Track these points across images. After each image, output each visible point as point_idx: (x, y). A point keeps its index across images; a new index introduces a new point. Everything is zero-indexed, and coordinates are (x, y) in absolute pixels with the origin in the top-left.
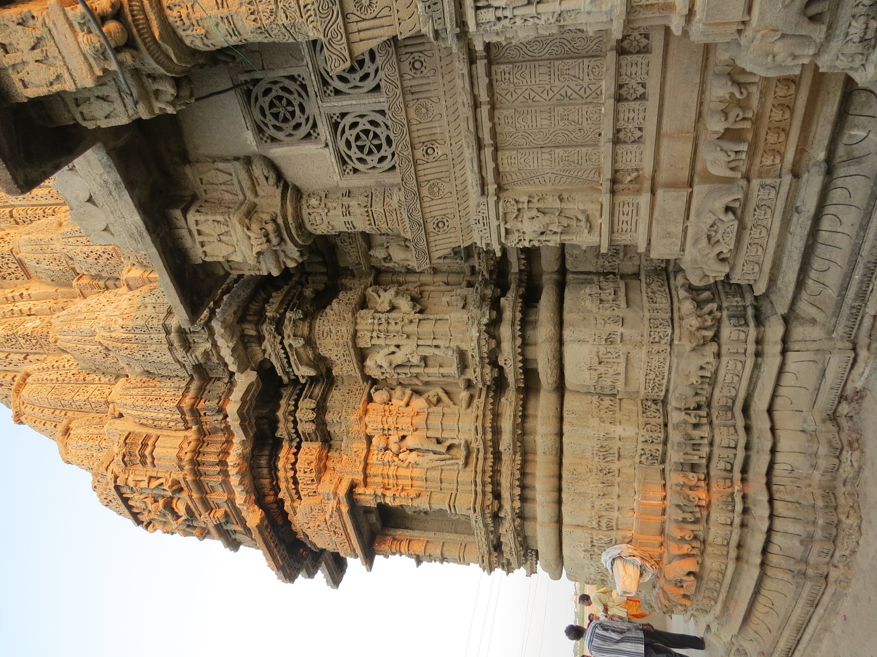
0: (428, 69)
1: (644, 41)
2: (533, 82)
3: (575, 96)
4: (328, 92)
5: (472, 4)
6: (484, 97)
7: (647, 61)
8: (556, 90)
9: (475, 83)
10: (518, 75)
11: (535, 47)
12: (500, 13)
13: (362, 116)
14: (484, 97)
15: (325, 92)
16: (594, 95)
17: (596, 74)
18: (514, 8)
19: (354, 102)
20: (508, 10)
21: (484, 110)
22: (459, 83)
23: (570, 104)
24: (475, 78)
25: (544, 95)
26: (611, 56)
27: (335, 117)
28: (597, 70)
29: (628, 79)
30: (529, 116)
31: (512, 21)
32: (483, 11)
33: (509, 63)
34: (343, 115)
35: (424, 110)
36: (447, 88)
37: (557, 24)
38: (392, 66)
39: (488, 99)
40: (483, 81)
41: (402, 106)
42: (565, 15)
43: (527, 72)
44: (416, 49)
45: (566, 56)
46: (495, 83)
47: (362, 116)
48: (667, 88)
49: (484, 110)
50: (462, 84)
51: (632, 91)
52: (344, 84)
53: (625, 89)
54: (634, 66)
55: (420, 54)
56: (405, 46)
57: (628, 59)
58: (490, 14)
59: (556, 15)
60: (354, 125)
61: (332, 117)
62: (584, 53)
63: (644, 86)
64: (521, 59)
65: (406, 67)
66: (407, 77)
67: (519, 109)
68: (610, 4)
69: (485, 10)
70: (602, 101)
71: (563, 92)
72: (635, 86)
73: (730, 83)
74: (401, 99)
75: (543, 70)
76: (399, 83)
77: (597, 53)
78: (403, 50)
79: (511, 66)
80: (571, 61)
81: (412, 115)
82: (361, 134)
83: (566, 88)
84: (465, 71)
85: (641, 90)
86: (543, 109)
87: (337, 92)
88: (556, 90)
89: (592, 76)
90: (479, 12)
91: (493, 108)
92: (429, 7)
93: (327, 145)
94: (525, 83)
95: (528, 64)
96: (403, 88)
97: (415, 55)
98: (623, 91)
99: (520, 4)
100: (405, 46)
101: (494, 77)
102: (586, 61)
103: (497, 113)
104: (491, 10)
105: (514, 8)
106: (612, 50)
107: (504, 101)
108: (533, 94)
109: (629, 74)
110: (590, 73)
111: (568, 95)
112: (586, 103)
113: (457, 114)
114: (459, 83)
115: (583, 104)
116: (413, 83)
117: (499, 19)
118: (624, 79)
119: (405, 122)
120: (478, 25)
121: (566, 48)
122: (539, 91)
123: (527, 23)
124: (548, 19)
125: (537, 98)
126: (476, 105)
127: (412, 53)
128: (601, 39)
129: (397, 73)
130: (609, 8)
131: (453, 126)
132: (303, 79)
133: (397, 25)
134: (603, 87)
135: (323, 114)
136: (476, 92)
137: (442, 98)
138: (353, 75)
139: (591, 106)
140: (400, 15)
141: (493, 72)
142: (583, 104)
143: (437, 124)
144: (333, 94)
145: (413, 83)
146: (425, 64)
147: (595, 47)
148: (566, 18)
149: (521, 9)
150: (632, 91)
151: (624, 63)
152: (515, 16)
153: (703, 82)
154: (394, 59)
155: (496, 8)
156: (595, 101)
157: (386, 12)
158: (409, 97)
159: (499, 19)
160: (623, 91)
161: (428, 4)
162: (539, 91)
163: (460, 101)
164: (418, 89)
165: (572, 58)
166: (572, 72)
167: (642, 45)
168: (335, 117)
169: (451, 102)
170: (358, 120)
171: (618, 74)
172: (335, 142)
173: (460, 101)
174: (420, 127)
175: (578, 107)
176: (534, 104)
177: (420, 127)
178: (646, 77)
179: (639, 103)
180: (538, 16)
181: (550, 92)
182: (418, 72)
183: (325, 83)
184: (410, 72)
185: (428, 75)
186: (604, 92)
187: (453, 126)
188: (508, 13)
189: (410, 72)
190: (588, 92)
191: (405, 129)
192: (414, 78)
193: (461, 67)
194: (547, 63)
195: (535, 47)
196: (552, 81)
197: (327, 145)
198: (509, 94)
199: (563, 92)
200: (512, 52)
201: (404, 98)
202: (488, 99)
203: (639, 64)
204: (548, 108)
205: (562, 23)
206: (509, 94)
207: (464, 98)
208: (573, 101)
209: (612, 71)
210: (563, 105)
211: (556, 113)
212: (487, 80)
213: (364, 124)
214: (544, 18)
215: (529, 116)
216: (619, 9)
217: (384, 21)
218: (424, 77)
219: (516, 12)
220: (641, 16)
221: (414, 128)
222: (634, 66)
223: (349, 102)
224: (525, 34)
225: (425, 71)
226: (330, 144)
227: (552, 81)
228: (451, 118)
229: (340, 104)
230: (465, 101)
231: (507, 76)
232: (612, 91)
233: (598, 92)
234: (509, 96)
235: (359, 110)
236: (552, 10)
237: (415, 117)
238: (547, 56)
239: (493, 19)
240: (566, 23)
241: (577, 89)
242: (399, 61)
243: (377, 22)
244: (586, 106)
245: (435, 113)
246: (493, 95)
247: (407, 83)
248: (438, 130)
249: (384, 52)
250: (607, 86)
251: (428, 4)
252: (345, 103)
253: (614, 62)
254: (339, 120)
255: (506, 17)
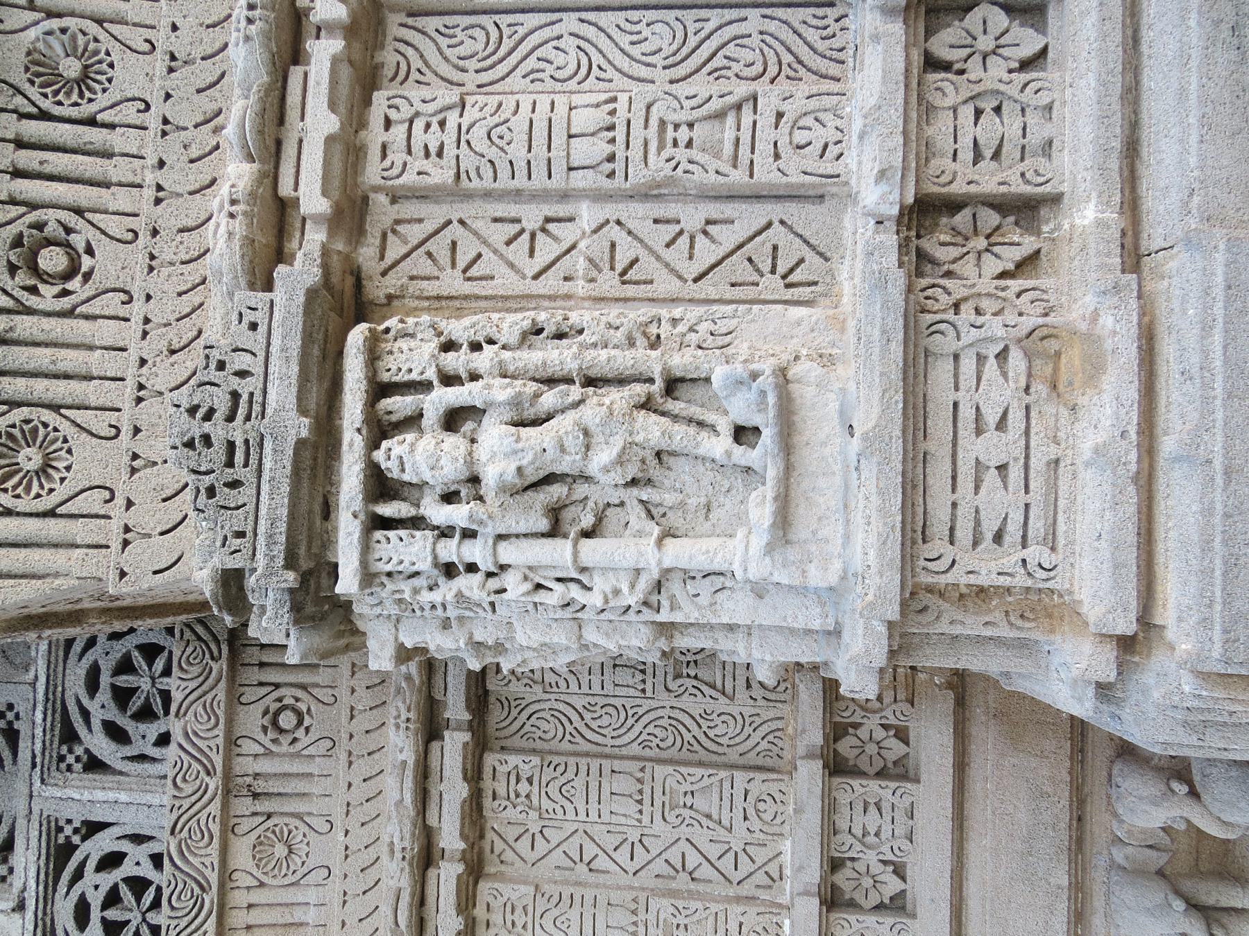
0: (313, 736)
1: (896, 749)
2: (594, 816)
3: (706, 871)
4: (70, 759)
5: (358, 504)
6: (450, 838)
7: (907, 800)
8: (655, 847)
9: (434, 793)
10: (553, 789)
11: (605, 721)
12: (449, 550)
13: (138, 839)
14: (450, 838)
15: (62, 758)
16: (760, 878)
17: (768, 817)
18: (500, 537)
19: (123, 797)
20: (479, 541)
21: (448, 875)
22: (390, 783)
23: (692, 895)
24: (434, 777)
25: (622, 856)
26: (810, 774)
27: (68, 830)
28: (769, 808)
29: (858, 846)
30: (574, 914)
31: (493, 584)
32: (392, 534)
33: (534, 751)
34: (93, 828)
35: (280, 850)
36: (357, 795)
37: (648, 615)
38: (210, 711)
39: (462, 845)
40: (452, 789)
41: (215, 828)
42: (674, 586)
43: (579, 783)
44: (291, 678)
45: (685, 754)
46: (487, 802)
47: (138, 839)
48: (972, 888)
49: (448, 875)
50: (397, 791)
51: (867, 882)
52: (114, 746)
53: (847, 872)
54: (872, 809)
55: (300, 693)
56: (262, 665)
57: (854, 790)
58: (415, 548)
59: (643, 584)
60: (112, 861)
61: (60, 829)
62: (733, 756)
63: (899, 871)
64: (565, 746)
65: (251, 720)
66: (248, 747)
67: (546, 888)
68: (837, 565)
69: (403, 533)
70: (785, 900)
71: (674, 856)
72: (877, 868)
73: (1179, 905)
74: (214, 809)
75: (624, 784)
76: (218, 761)
77: (769, 762)
78: (255, 675)
79: (536, 760)
80: (699, 772)
81: (242, 856)
82: (125, 891)
83: (683, 845)
84: (409, 756)
85: (892, 885)
86: (615, 897)
87: (94, 765)
88: (655, 847)
89: (756, 824)
90: (378, 535)
91: (474, 869)
92: (211, 492)
93: (21, 907)
94: (571, 815)
95: (583, 762)
96: (228, 775)
97: (282, 691)
98: (842, 879)
99: (522, 528)
100: (262, 665)
101: (487, 784)
102: (740, 777)
103: (484, 887)
104: (423, 539)
105: (500, 537)
106: (810, 756)
107: (509, 855)
108: (590, 850)
109: (858, 831)
110: (751, 812)
111: (690, 866)
112: (738, 899)
113: (372, 875)
114: (390, 783)
115: (728, 900)
116: (264, 766)
117: (449, 570)
118: (846, 845)
119: (214, 878)
120: (368, 578)
121: (687, 736)
122: (610, 842)
123: (541, 596)
124: (617, 592)
125: (602, 862)
126: (427, 856)
127: (277, 686)
128: (780, 724)
129: (220, 731)
130: (833, 579)
131: (357, 907)
132: (17, 717)
133: (116, 545)
134: (787, 859)
135: (35, 816)
136: (432, 821)
137: (338, 823)
138: (142, 727)
139: (752, 910)
140: (132, 518)
141: (487, 771)
142: (728, 900)
143: (311, 896)
144: (78, 767)
145: (264, 766)
146: (307, 721)
147: (764, 745)
148: (681, 598)
149: (524, 543)
150: (867, 882)
151: (843, 798)
152: (503, 568)
153: (1079, 888)
154: (221, 692)
155: (445, 532)
156: (764, 895)
157: (92, 502)
158: (243, 805)
159: (449, 570)
160: (842, 879)
161: (207, 480)
162: (610, 842)
163: (386, 839)
164: (274, 787)
165: (700, 764)
166: (699, 803)
167: (891, 756)
168: (68, 830)
169: (360, 836)
170: (125, 846)
171: (830, 829)
172: (47, 899)
173: (386, 839)
174: (255, 897)
175: (714, 907)
176: (592, 878)
177: (255, 897)
178: (906, 845)
179: (890, 921)
180: (579, 578)
181: (638, 849)
182: (285, 740)
183: (70, 737)
184: (260, 737)
185: (311, 750)
186: (787, 872)
187: (357, 907)
188: (476, 552)
189: (260, 737)
190: (745, 866)
191: (210, 898)
192: (269, 753)
193: (400, 745)
194: (634, 766)
195: (605, 721)
196: (646, 819)
197: (21, 907)
198: (526, 841)
199: (674, 856)
200: (544, 725)
201: (225, 806)
202: (462, 845)
203: (886, 807)
204: (629, 895)
205: (664, 616)
206: (526, 841)
207: (397, 830)
208: (701, 887)
209: (813, 817)
210: (673, 894)
211: (651, 917)
212: (463, 790)
213: (137, 863)
214: (601, 584)
215: (574, 914)
216: (874, 581)
217: (80, 530)
218: (298, 755)
219: (507, 553)
220: (944, 627)
221: (239, 898)
222: (872, 809)
223: (111, 796)
224: (536, 639)
225: (305, 741)
226: (31, 904)
227: (646, 819)
228: (355, 885)
229: (87, 796)
230: (396, 841)
231: (524, 787)
232: (813, 874)
233: (773, 869)
234: (523, 846)
235: (134, 821)
236: (631, 563)
237: (250, 865)
238: (635, 749)
239: (425, 565)
240: (678, 617)
241: (713, 851)
242: (235, 700)
243: (53, 529)
244: (741, 909)
245: (311, 863)
246: (482, 837)
247: (245, 765)
248: (311, 916)
249: (195, 670)
250: (798, 857)
251: (207, 480)
252: (100, 795)
253: (818, 791)
254: (76, 839)
255: (472, 568)
